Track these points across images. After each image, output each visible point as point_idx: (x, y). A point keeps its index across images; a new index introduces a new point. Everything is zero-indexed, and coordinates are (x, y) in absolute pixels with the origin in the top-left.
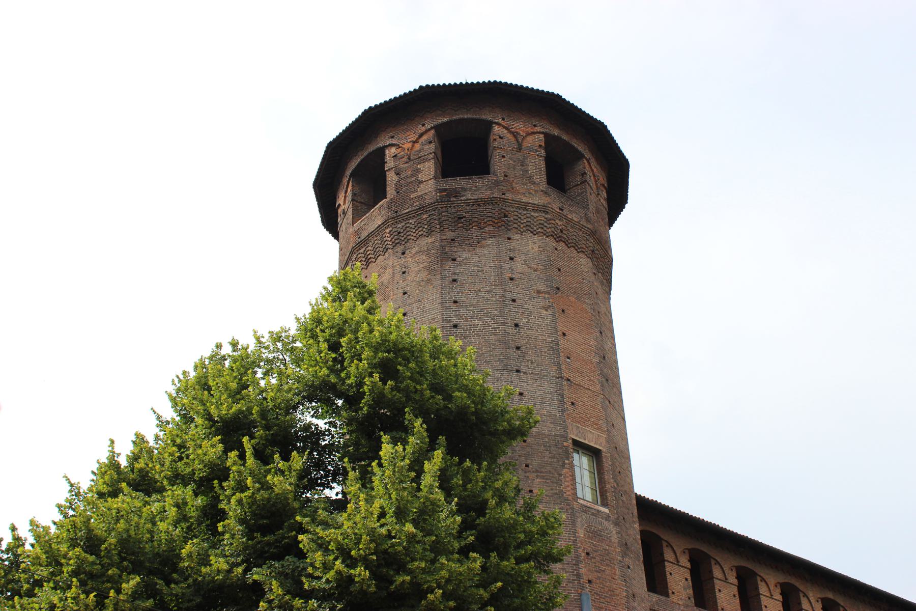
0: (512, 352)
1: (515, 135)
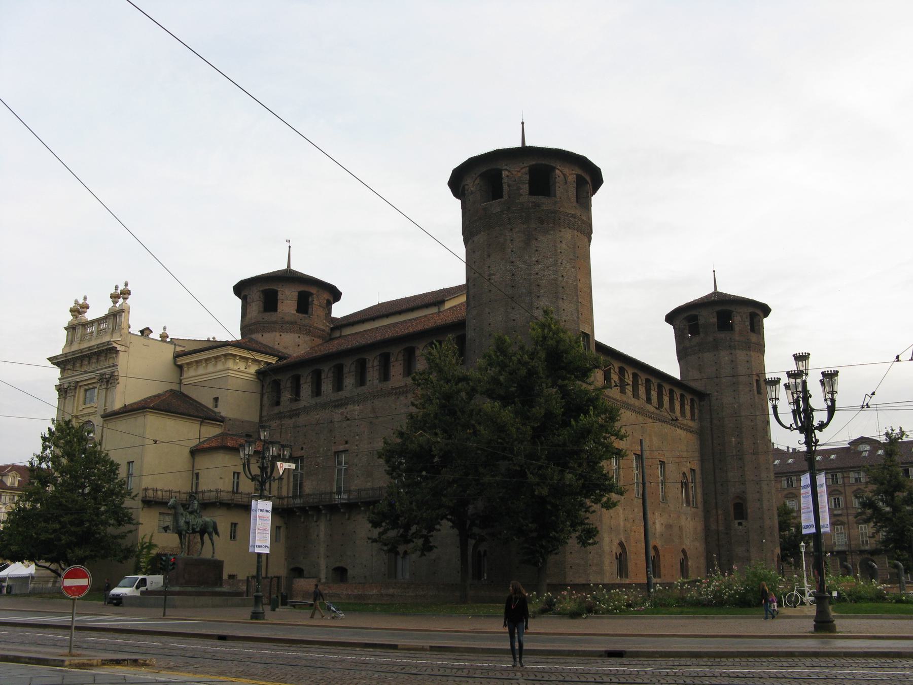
0: (561, 290)
1: (564, 175)
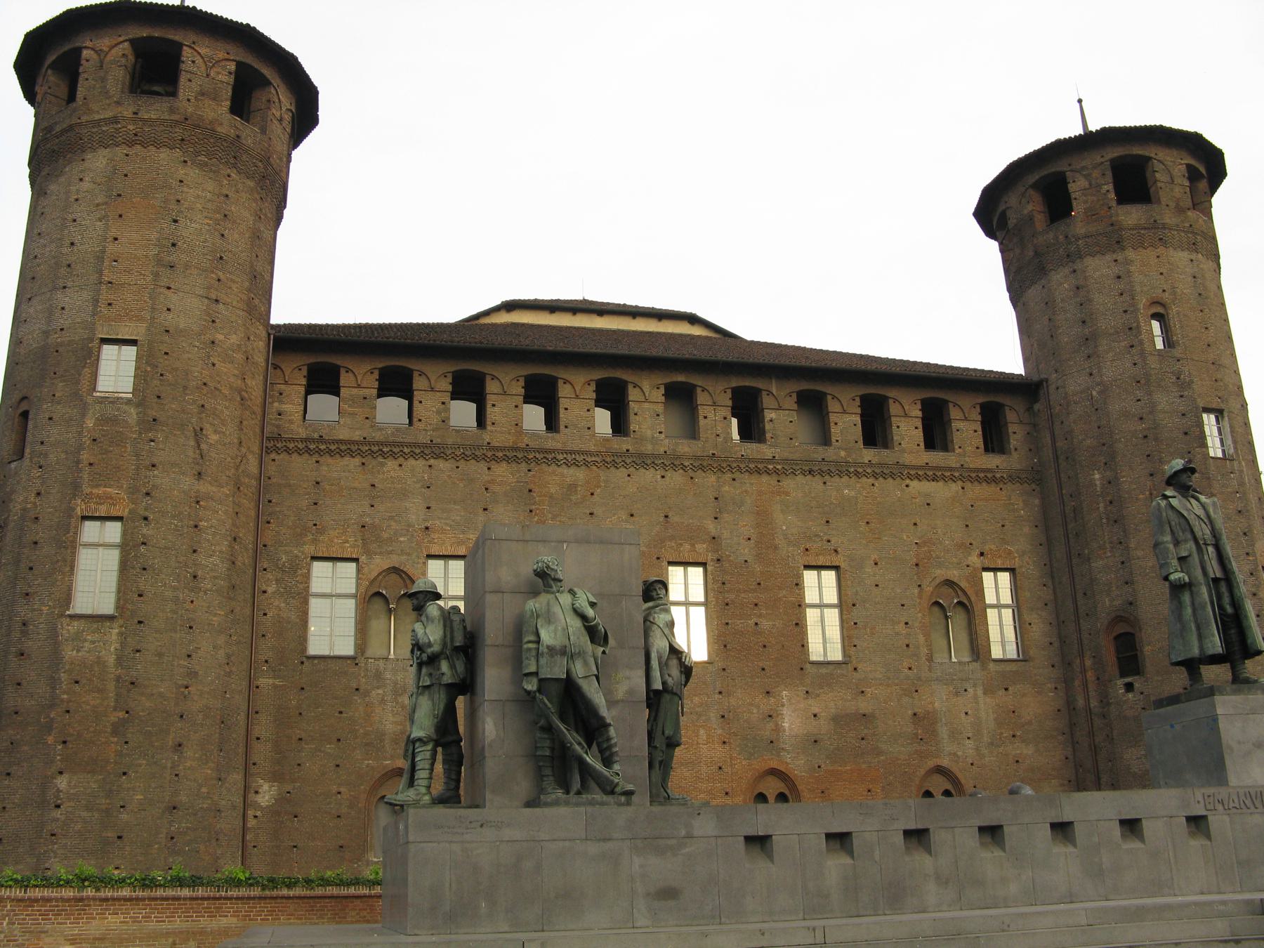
0: (63, 271)
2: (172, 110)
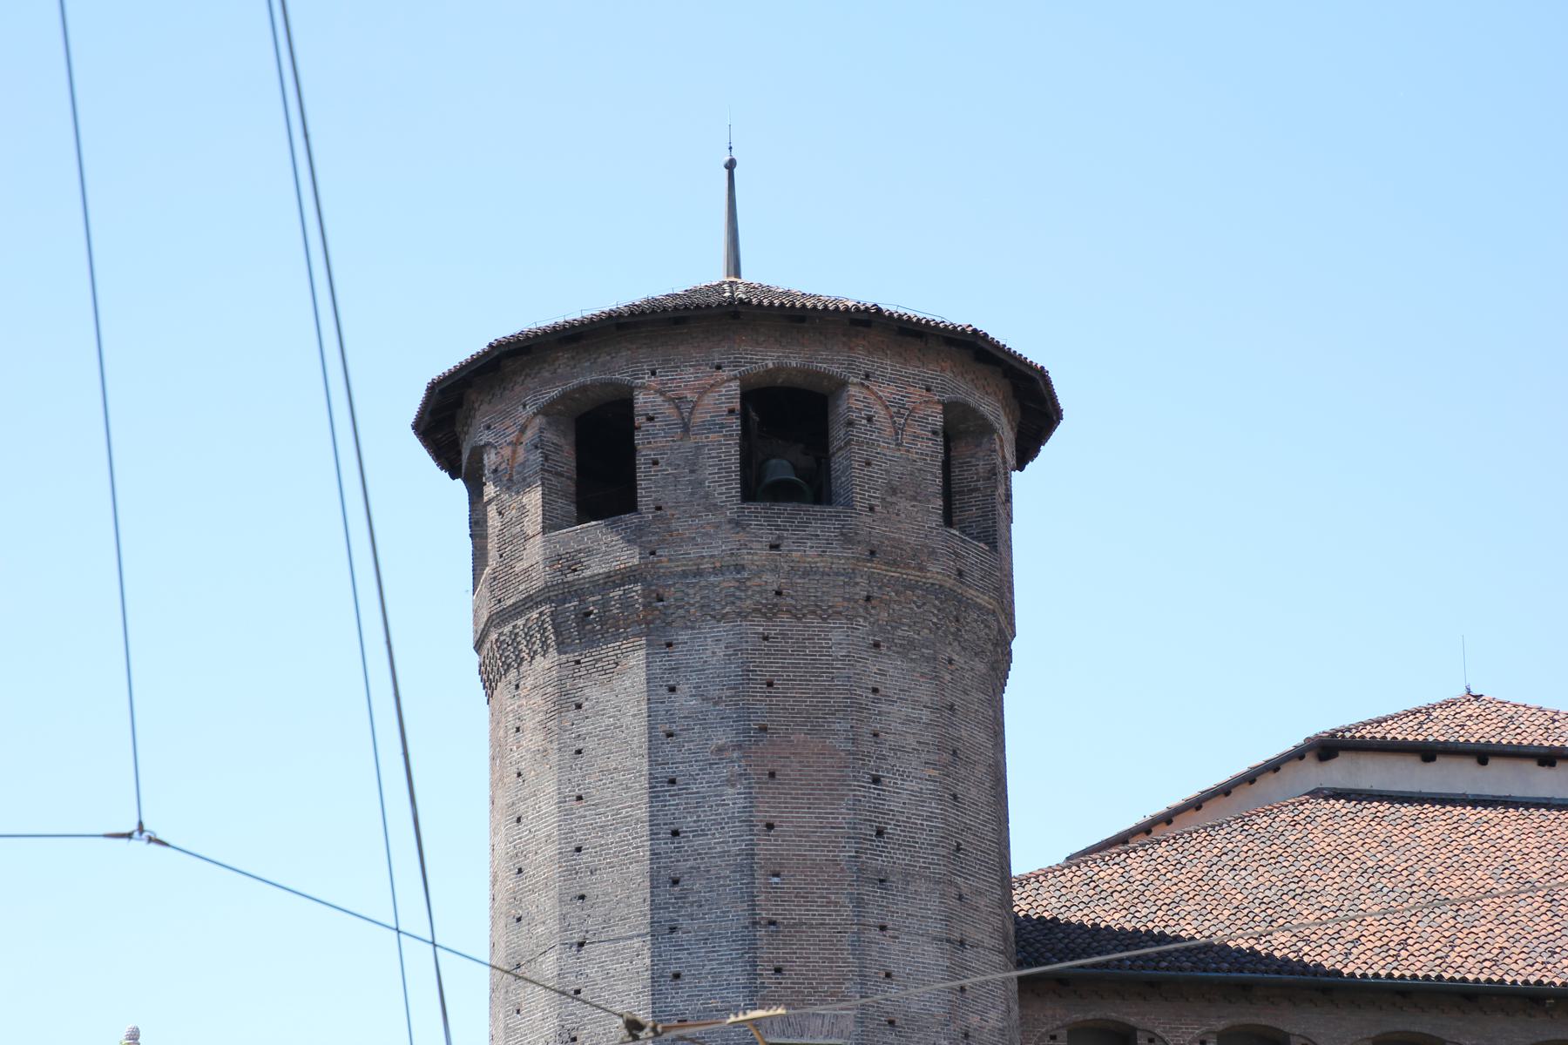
1: (677, 402)
2: (847, 539)
